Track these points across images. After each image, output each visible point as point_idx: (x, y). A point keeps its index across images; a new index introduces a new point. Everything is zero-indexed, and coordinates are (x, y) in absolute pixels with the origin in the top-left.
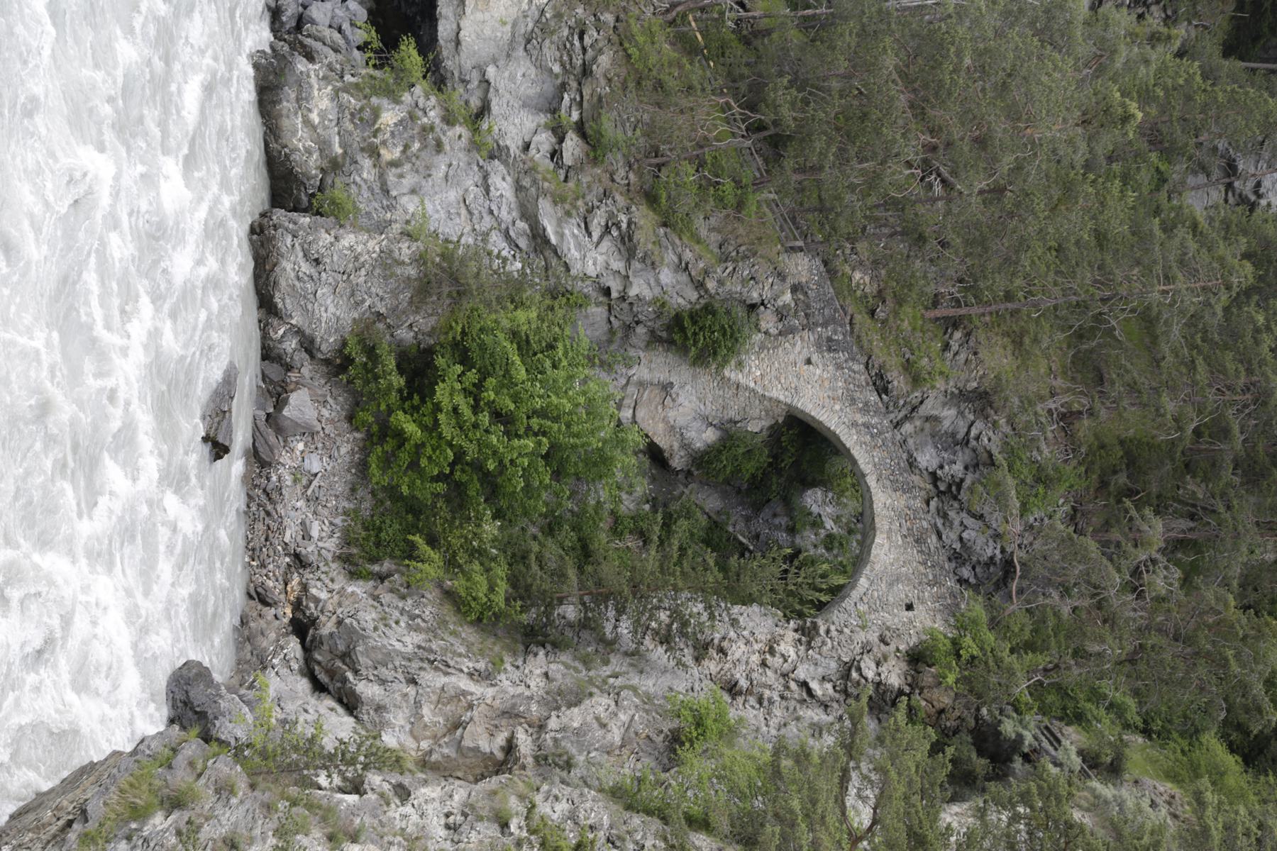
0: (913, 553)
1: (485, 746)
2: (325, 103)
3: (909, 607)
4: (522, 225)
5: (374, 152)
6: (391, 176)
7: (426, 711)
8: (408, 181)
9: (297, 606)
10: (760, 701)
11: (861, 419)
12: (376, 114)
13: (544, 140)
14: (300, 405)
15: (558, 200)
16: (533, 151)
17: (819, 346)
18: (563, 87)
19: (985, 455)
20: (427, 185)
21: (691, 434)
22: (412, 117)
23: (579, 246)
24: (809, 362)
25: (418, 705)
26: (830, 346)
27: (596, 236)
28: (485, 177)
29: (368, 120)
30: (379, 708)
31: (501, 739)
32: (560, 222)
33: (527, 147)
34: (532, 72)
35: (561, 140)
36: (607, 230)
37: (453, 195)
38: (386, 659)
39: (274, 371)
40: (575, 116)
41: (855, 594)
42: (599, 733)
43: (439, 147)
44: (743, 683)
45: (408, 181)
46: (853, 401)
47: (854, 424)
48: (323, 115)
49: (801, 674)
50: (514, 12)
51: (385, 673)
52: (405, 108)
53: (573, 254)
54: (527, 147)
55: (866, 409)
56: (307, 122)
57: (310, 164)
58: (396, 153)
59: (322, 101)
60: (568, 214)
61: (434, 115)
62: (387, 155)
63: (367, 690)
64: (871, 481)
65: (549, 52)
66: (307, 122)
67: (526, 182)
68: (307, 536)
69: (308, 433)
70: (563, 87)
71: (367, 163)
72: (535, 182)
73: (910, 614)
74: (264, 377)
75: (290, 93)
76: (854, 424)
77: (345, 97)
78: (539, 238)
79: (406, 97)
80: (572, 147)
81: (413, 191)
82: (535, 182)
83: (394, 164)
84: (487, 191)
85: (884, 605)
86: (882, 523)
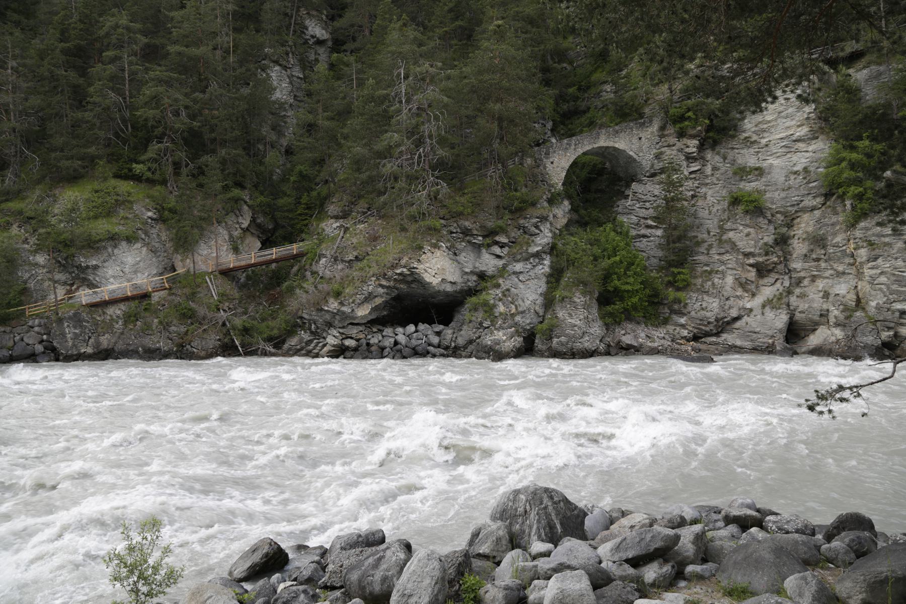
0: (621, 135)
1: (754, 274)
2: (501, 333)
3: (640, 139)
4: (531, 260)
5: (513, 315)
6: (520, 309)
7: (738, 294)
8: (520, 302)
9: (688, 341)
10: (698, 187)
11: (573, 147)
12: (501, 314)
13: (497, 250)
14: (627, 340)
15: (528, 244)
16: (502, 254)
17: (547, 158)
18: (469, 242)
19: (583, 108)
20: (520, 296)
21: (567, 210)
22: (500, 300)
23: (543, 238)
24: (552, 163)
25: (737, 297)
26: (547, 154)
27: (537, 231)
28: (514, 273)
29: (505, 316)
30: (740, 309)
31: (750, 268)
32: (536, 245)
33: (498, 257)
34: (464, 254)
35: (497, 243)
36: (537, 227)
37: (521, 286)
38: (722, 307)
39: (613, 351)
40: (480, 238)
41: (635, 156)
42: (753, 236)
43: (508, 290)
44: (692, 193)
45: (520, 302)
46: (566, 149)
47: (575, 149)
48: (504, 335)
49: (686, 173)
50: (447, 259)
51: (726, 307)
52: (497, 302)
53: (545, 240)
54: (498, 257)
55: (570, 145)
56: (504, 342)
57: (517, 341)
58: (513, 306)
59: (500, 335)
60: (533, 241)
61: (498, 292)
62: (513, 311)
63: (734, 313)
64: (596, 146)
65: (458, 246)
66: (504, 342)
67: (519, 257)
68: (664, 338)
69: (636, 337)
70: (469, 242)
71: (518, 318)
72: (521, 254)
73: (643, 139)
74: (617, 354)
75: (497, 347)
76: (575, 149)
77: (497, 326)
78: (537, 255)
79: (492, 302)
80: (503, 239)
81: (523, 301)
82: (521, 254)
83: (516, 306)
84: (521, 272)
85: (640, 147)
86: (611, 144)
